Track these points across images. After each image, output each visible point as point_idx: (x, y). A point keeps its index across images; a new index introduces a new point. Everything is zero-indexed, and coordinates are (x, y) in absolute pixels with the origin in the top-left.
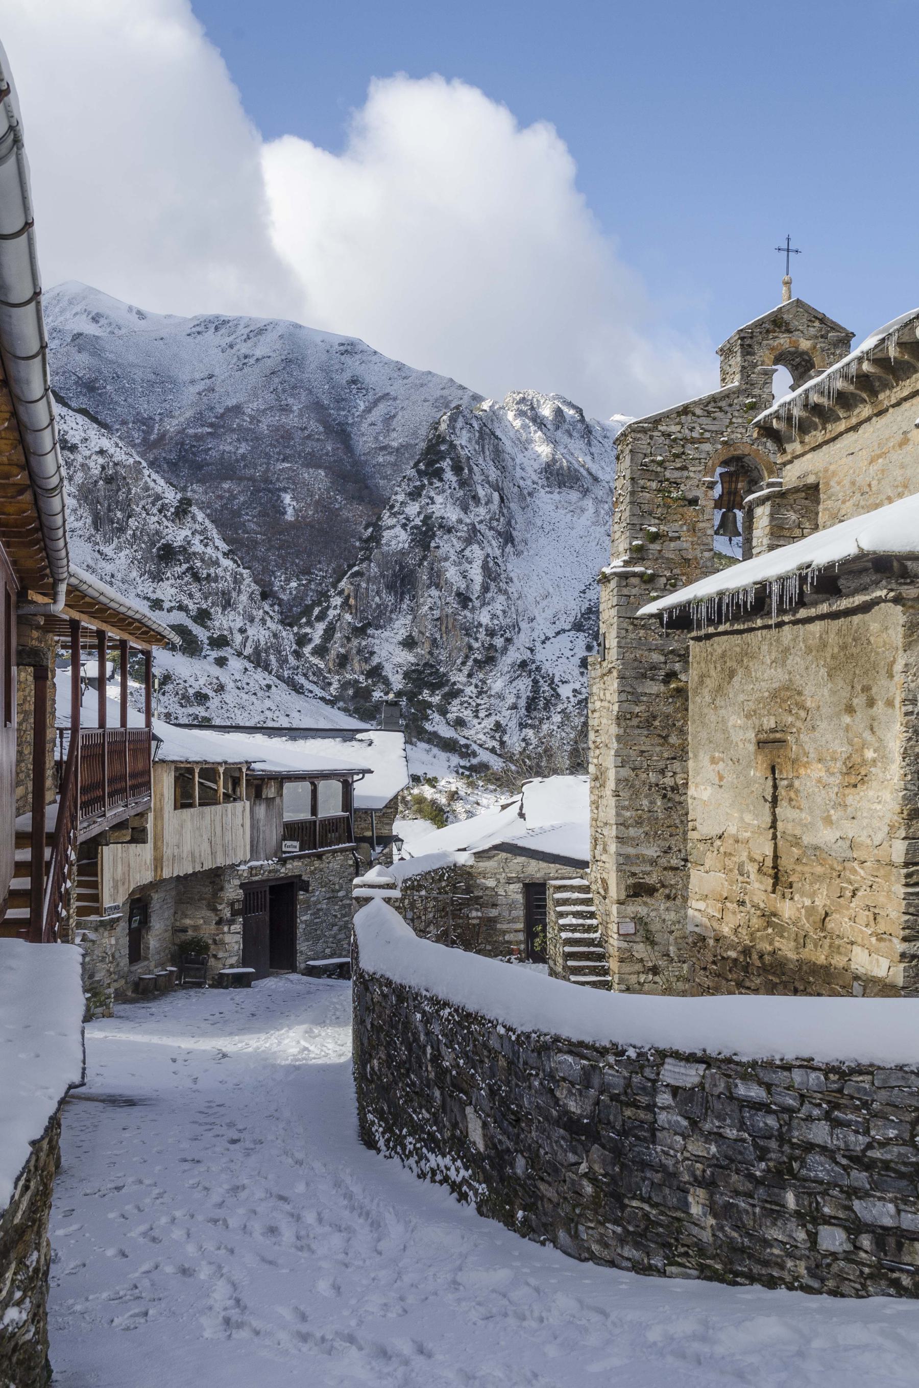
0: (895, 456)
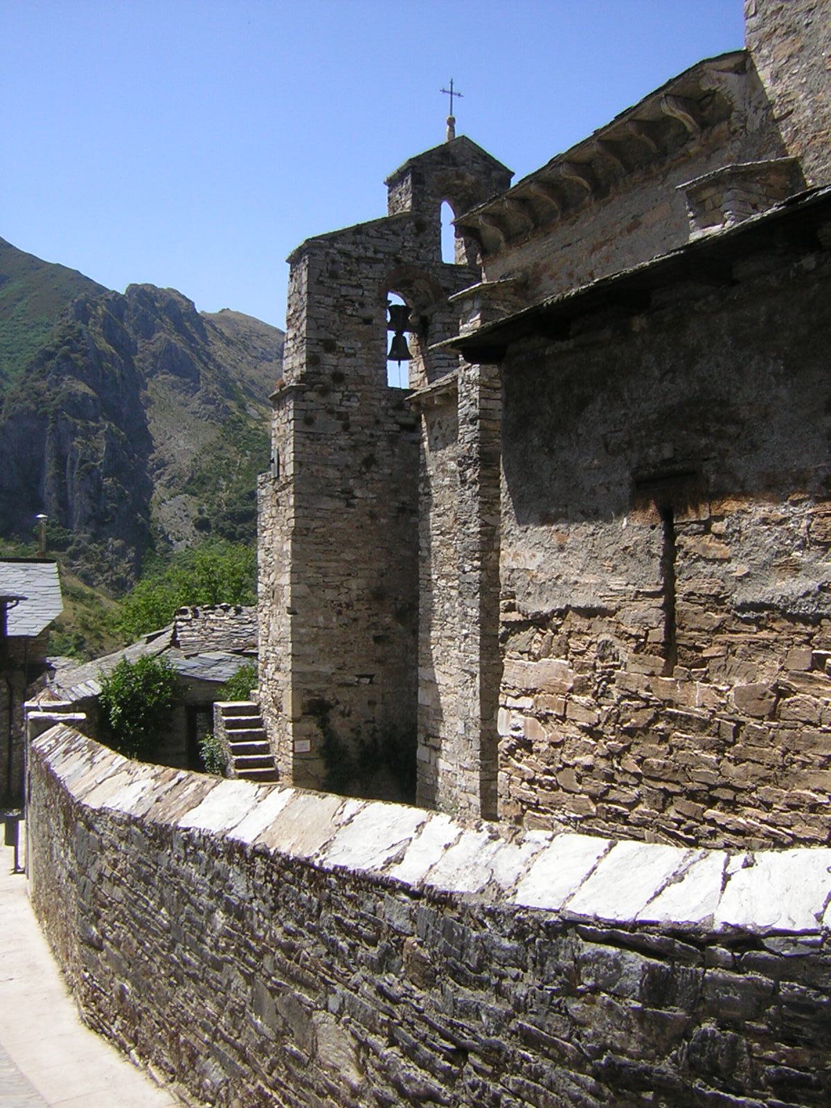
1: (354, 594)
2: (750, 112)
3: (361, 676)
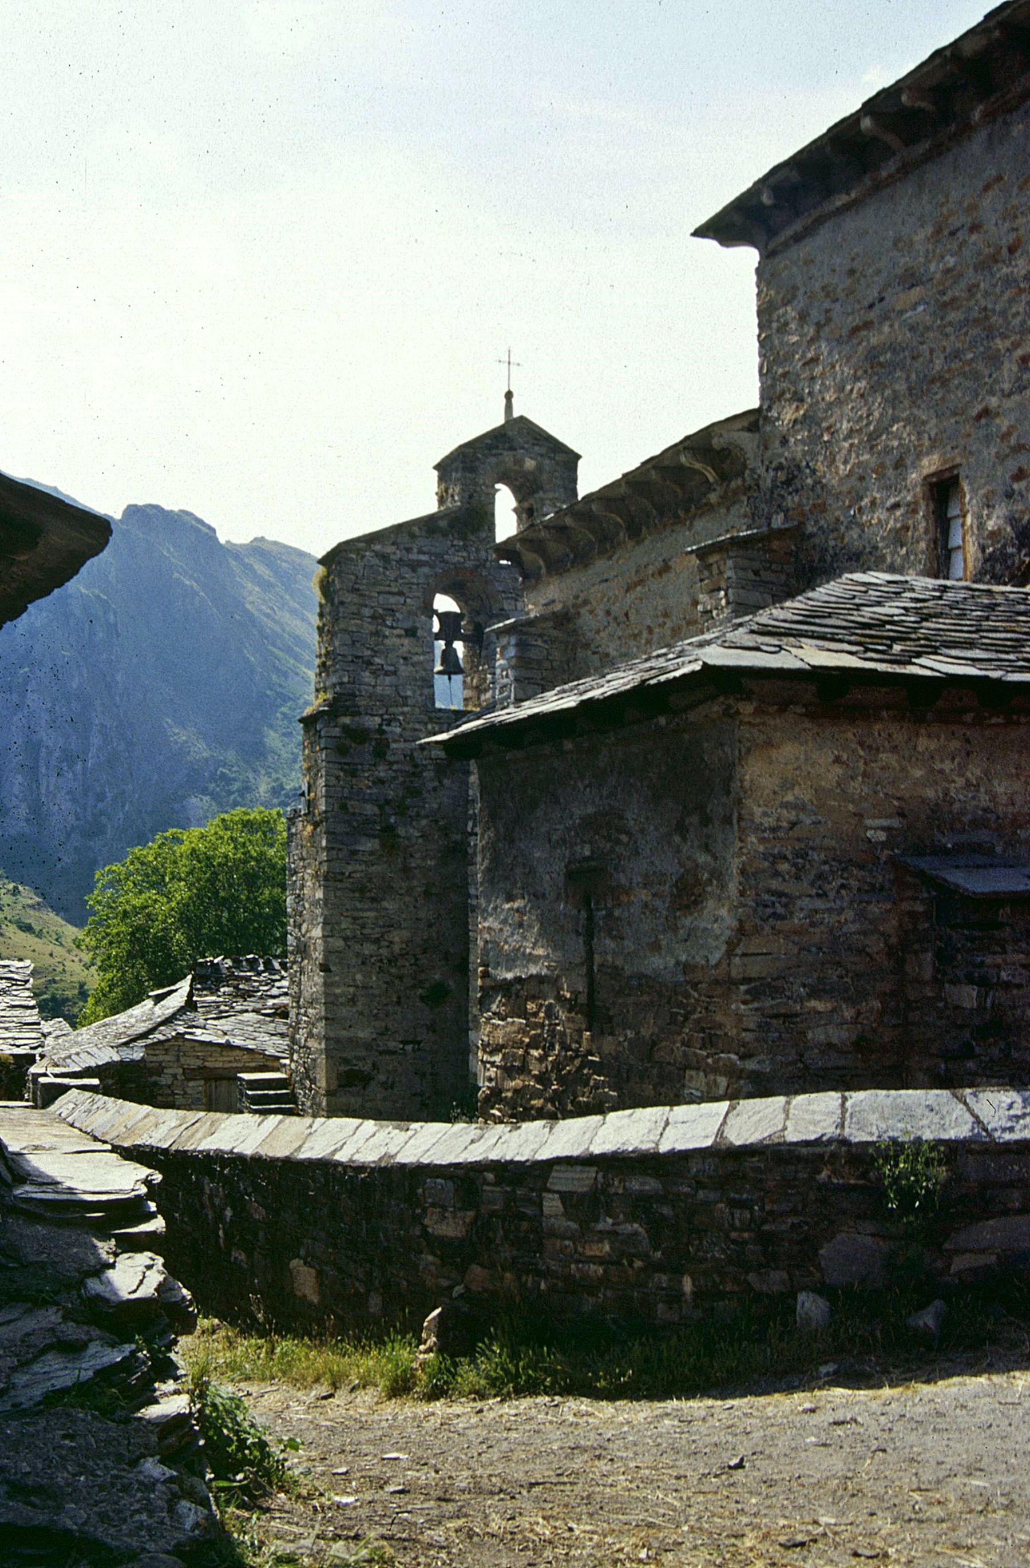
0: (654, 585)
1: (396, 948)
2: (761, 471)
3: (405, 1043)
